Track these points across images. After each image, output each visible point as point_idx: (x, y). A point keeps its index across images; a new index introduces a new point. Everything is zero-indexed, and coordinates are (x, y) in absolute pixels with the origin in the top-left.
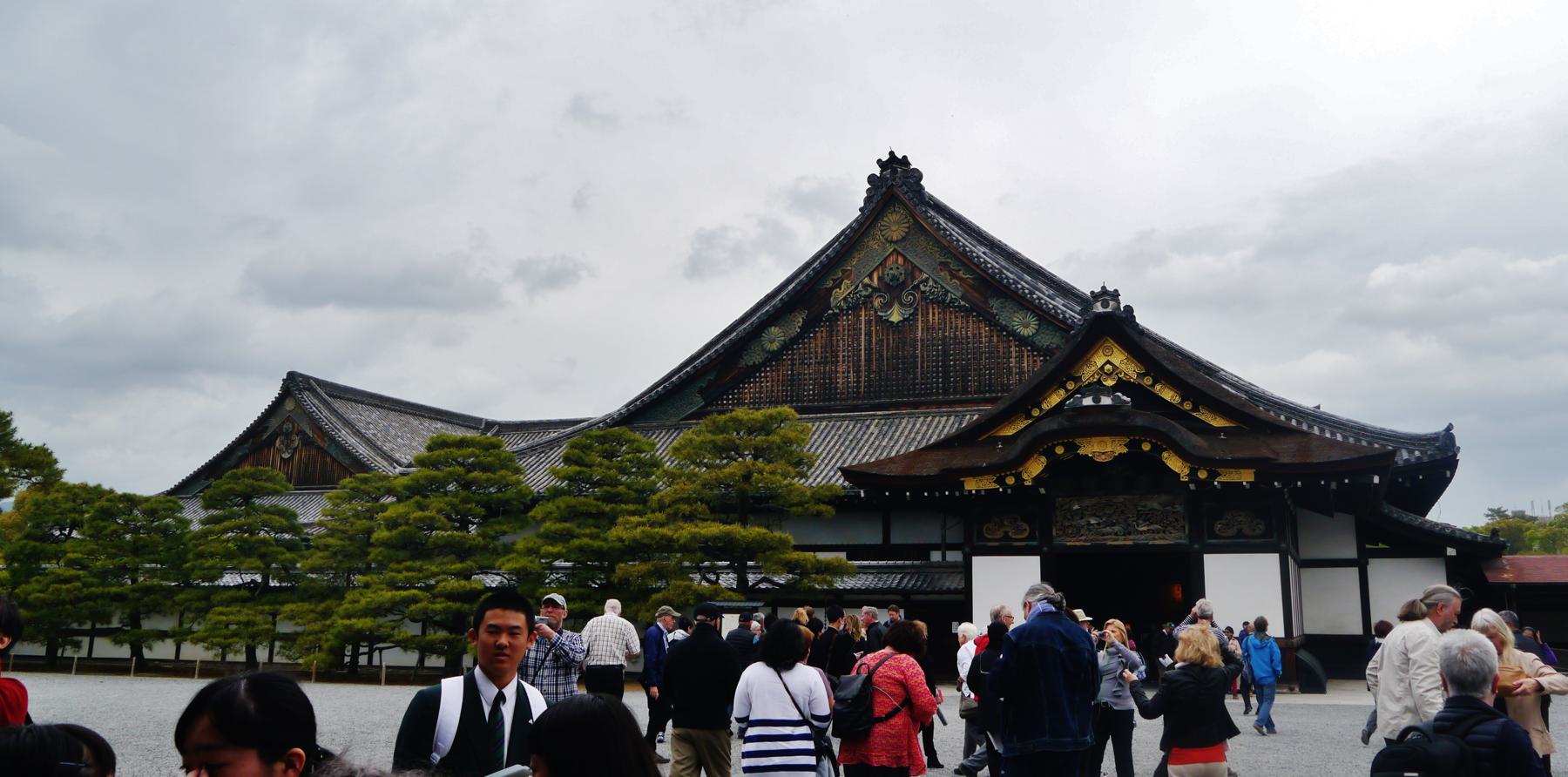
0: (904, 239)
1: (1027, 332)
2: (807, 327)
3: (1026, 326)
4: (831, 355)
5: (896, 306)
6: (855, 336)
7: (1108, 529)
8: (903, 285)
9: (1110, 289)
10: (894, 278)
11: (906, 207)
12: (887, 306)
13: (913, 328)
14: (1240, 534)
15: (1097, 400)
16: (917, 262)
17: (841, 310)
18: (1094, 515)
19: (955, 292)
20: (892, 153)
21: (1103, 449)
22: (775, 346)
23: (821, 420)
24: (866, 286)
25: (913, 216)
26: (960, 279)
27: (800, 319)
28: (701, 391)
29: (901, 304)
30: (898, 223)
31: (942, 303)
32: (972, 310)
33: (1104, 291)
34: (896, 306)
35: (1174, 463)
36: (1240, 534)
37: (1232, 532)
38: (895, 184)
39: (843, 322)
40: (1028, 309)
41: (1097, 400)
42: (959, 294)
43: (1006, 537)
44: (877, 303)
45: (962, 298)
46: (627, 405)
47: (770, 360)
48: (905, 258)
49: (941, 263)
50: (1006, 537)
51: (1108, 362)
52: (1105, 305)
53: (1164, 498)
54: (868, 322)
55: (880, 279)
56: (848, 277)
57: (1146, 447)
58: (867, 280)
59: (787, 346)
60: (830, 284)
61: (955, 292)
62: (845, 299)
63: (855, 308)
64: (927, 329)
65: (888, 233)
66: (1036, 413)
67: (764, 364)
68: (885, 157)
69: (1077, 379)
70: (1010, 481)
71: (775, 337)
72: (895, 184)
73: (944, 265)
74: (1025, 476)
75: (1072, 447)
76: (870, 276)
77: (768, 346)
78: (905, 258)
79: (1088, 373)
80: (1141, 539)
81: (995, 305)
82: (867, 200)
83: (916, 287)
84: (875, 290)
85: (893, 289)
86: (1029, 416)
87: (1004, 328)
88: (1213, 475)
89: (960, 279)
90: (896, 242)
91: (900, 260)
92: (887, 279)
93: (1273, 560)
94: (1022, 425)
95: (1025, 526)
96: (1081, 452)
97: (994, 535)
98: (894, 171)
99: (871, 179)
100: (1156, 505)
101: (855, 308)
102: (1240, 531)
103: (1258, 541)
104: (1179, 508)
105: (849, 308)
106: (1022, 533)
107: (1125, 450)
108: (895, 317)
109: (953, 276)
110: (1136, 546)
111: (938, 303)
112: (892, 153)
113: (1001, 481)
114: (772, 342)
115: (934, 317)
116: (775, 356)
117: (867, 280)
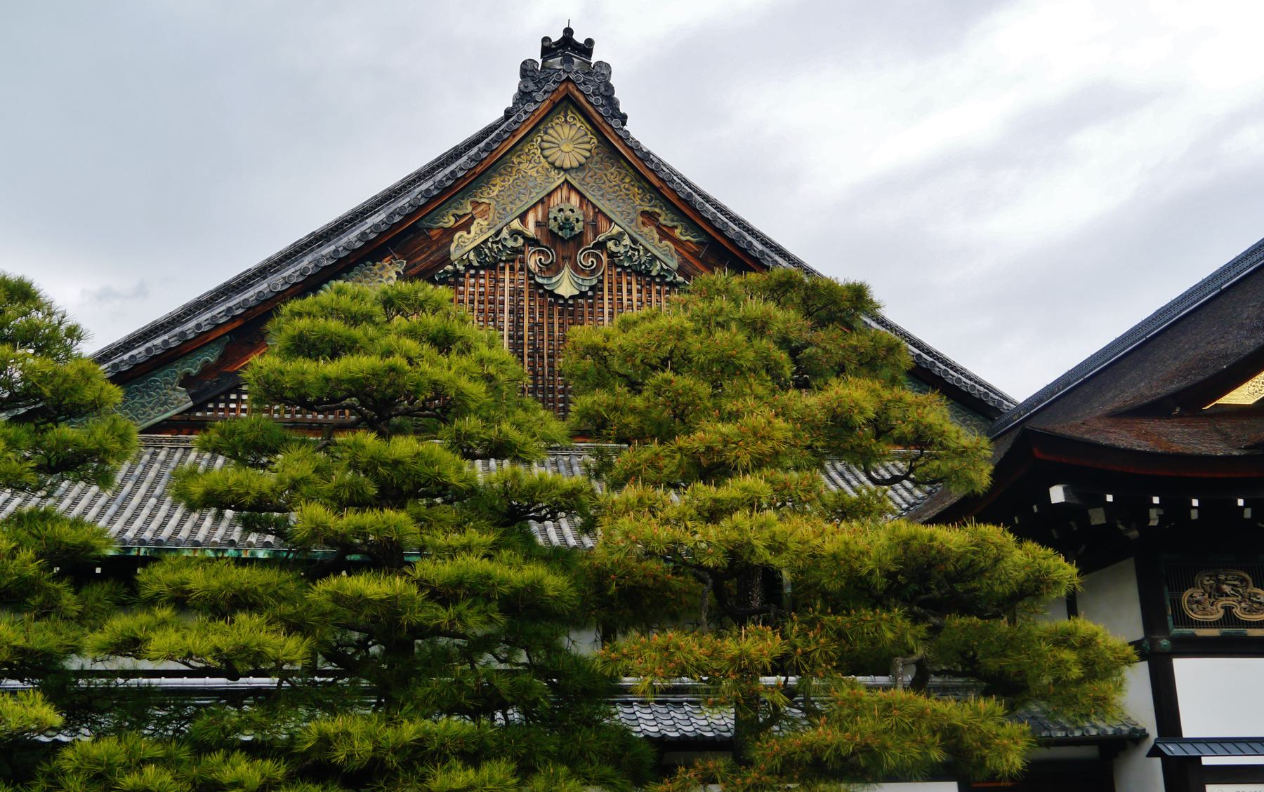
0: (581, 165)
5: (567, 271)
10: (566, 224)
11: (588, 118)
17: (469, 266)
20: (568, 31)
24: (515, 234)
25: (597, 131)
26: (676, 241)
28: (187, 381)
29: (576, 269)
31: (641, 273)
34: (567, 271)
39: (470, 286)
42: (674, 265)
43: (1229, 618)
44: (533, 262)
48: (582, 196)
49: (644, 213)
50: (1229, 618)
54: (516, 293)
55: (537, 224)
58: (516, 224)
60: (450, 221)
62: (475, 249)
68: (556, 36)
73: (650, 217)
76: (523, 217)
78: (582, 196)
82: (524, 96)
83: (601, 245)
84: (530, 241)
85: (562, 242)
89: (676, 241)
90: (566, 171)
91: (575, 199)
92: (553, 225)
97: (1204, 608)
98: (568, 60)
99: (526, 70)
101: (492, 266)
105: (483, 266)
108: (566, 286)
109: (665, 234)
112: (568, 31)
117: (516, 224)
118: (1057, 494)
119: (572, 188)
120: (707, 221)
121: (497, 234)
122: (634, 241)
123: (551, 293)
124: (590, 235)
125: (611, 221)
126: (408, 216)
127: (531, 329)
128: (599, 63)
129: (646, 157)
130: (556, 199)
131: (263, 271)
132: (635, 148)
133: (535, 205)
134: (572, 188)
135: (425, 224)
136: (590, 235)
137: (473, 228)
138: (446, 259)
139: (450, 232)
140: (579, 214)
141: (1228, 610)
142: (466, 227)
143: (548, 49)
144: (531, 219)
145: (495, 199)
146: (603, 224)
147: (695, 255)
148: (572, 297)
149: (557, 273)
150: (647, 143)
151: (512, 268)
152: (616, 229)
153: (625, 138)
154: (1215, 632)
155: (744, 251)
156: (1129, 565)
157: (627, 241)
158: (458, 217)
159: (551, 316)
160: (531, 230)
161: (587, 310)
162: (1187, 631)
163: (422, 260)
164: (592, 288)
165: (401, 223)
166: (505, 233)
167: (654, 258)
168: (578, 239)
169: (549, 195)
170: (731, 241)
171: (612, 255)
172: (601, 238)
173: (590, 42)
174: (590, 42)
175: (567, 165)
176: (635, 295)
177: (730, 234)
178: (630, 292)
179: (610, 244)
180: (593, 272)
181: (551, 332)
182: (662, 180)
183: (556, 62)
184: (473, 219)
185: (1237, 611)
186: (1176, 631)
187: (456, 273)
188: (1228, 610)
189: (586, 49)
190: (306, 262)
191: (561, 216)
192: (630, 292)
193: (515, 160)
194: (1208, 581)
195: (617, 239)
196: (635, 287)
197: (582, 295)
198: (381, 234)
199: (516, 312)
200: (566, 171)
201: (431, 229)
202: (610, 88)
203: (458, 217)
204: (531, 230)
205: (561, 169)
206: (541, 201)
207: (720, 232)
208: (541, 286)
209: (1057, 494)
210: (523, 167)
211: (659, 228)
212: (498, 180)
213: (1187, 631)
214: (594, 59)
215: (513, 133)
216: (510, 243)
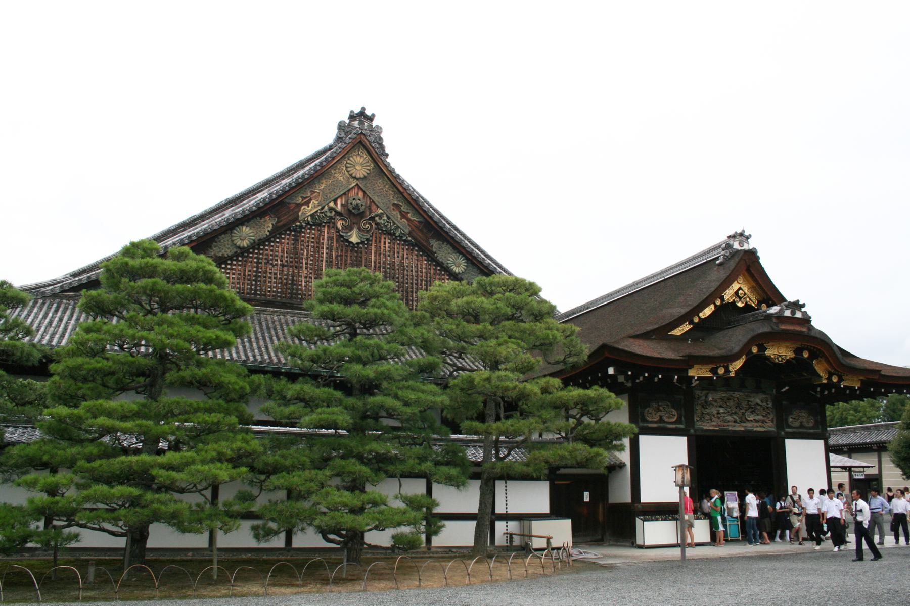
1: (456, 270)
2: (276, 233)
3: (458, 266)
4: (295, 261)
6: (318, 249)
7: (729, 418)
8: (361, 215)
9: (746, 234)
10: (357, 207)
12: (349, 228)
13: (368, 253)
14: (802, 426)
15: (793, 313)
16: (376, 199)
17: (308, 223)
18: (721, 406)
19: (403, 226)
20: (363, 109)
21: (779, 352)
22: (245, 244)
23: (285, 314)
24: (331, 209)
26: (409, 220)
27: (268, 224)
29: (359, 229)
30: (362, 164)
31: (389, 233)
32: (416, 245)
33: (741, 235)
35: (821, 368)
36: (802, 426)
37: (797, 424)
38: (360, 137)
39: (307, 234)
40: (460, 253)
41: (793, 313)
42: (407, 231)
43: (661, 420)
44: (339, 225)
45: (410, 234)
46: (75, 275)
47: (237, 256)
48: (364, 193)
49: (394, 204)
50: (661, 420)
51: (740, 289)
52: (741, 244)
53: (762, 396)
54: (330, 239)
55: (342, 205)
56: (316, 198)
57: (806, 355)
58: (332, 204)
59: (258, 245)
61: (403, 226)
63: (317, 223)
64: (378, 252)
65: (353, 171)
66: (696, 320)
67: (231, 258)
68: (357, 110)
69: (722, 299)
70: (721, 371)
71: (246, 235)
72: (360, 137)
74: (730, 368)
75: (762, 348)
76: (335, 201)
77: (239, 243)
79: (728, 295)
80: (749, 426)
81: (435, 245)
82: (339, 139)
83: (372, 219)
84: (338, 213)
85: (354, 215)
86: (691, 322)
87: (439, 264)
88: (841, 380)
89: (409, 220)
90: (357, 179)
91: (361, 195)
93: (820, 444)
94: (686, 327)
95: (674, 412)
96: (767, 353)
97: (652, 416)
99: (341, 126)
100: (759, 402)
102: (801, 423)
103: (812, 431)
104: (770, 405)
106: (671, 417)
107: (790, 355)
108: (354, 239)
109: (404, 215)
110: (747, 431)
111: (390, 234)
112: (363, 109)
113: (714, 371)
114: (242, 240)
115: (386, 244)
116: (243, 253)
117: (332, 204)
118: (611, 371)
119: (360, 188)
120: (424, 211)
121: (323, 208)
122: (388, 218)
123: (347, 241)
124: (368, 213)
125: (378, 207)
126: (280, 196)
127: (336, 258)
128: (377, 127)
129: (397, 177)
130: (352, 194)
131: (203, 217)
132: (392, 172)
133: (341, 196)
134: (360, 188)
135: (287, 201)
136: (368, 213)
137: (311, 205)
138: (296, 219)
139: (299, 206)
140: (363, 202)
141: (661, 417)
142: (307, 204)
143: (352, 117)
144: (339, 202)
145: (323, 191)
146: (374, 208)
147: (417, 227)
148: (358, 244)
149: (351, 230)
150: (393, 165)
151: (328, 227)
152: (380, 211)
153: (387, 166)
154: (655, 425)
155: (441, 228)
156: (626, 396)
157: (385, 218)
158: (303, 198)
159: (347, 251)
160: (339, 208)
161: (364, 250)
162: (645, 425)
163: (285, 220)
164: (367, 240)
165: (276, 199)
166: (326, 207)
167: (398, 227)
168: (361, 215)
169: (349, 191)
170: (436, 222)
171: (377, 224)
172: (373, 215)
173: (373, 115)
174: (373, 115)
175: (358, 176)
176: (387, 245)
177: (435, 219)
178: (385, 243)
179: (377, 218)
180: (368, 232)
181: (346, 260)
182: (405, 189)
183: (356, 124)
184: (311, 200)
185: (664, 418)
186: (641, 424)
187: (301, 227)
188: (661, 417)
189: (371, 119)
190: (228, 213)
191: (354, 202)
192: (385, 243)
193: (333, 172)
194: (655, 405)
195: (380, 216)
196: (388, 241)
197: (362, 243)
198: (266, 204)
199: (330, 249)
200: (357, 179)
201: (289, 203)
202: (381, 139)
203: (303, 198)
204: (339, 208)
205: (355, 178)
206: (345, 194)
207: (431, 217)
208: (342, 237)
209: (611, 371)
210: (336, 175)
211: (401, 212)
212: (324, 181)
213: (645, 425)
214: (374, 124)
215: (333, 158)
216: (328, 214)
